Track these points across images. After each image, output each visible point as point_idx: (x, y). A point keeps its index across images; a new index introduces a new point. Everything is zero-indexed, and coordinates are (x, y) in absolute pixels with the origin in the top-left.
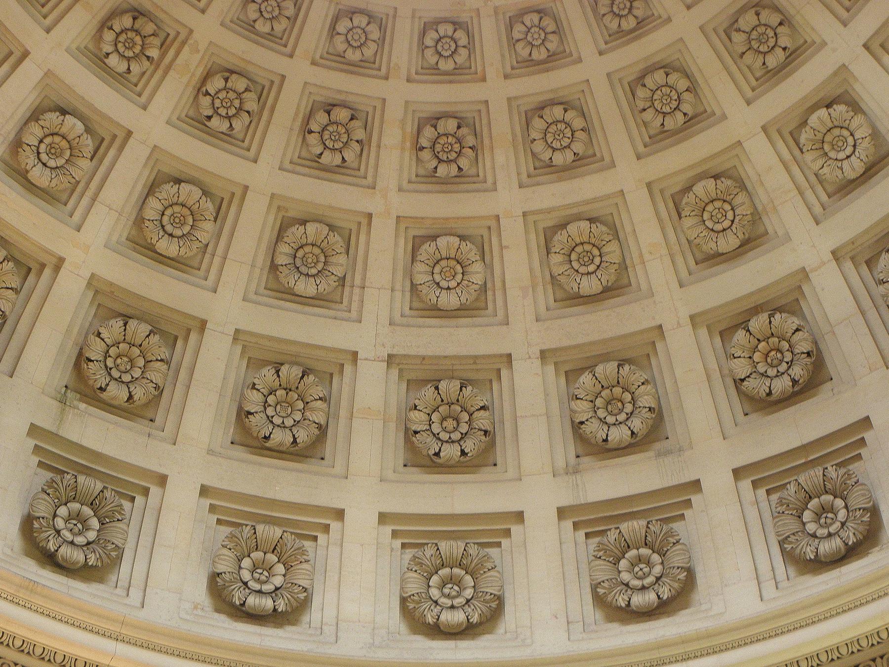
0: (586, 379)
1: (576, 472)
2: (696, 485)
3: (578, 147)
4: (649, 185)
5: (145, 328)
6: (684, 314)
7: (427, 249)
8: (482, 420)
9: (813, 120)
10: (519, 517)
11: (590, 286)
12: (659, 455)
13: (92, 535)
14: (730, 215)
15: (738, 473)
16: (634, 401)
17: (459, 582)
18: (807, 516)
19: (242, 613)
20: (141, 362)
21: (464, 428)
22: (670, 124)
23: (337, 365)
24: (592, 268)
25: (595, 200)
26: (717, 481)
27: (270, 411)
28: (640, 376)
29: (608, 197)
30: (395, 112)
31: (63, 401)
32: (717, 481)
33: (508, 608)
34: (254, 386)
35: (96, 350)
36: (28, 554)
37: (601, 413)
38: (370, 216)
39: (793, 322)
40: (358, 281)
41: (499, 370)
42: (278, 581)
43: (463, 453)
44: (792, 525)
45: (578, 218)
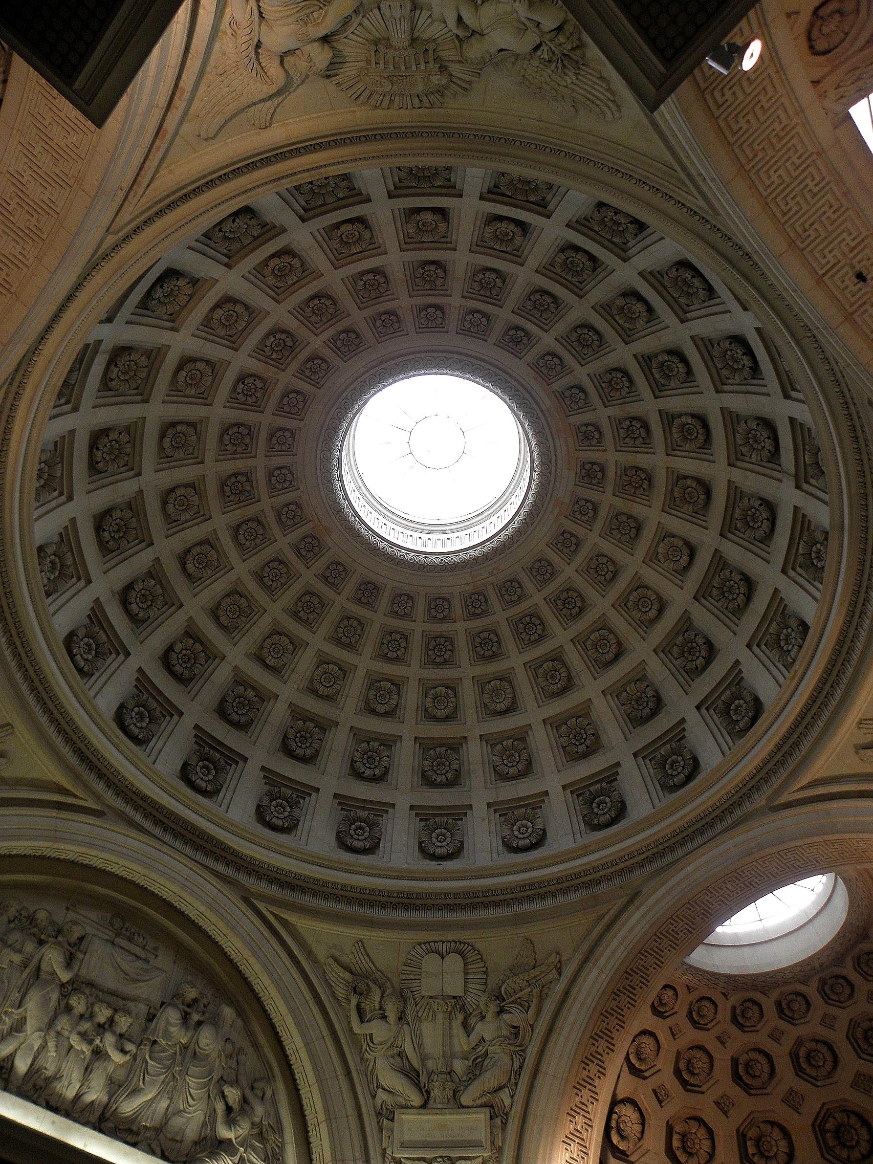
3: (248, 544)
9: (283, 638)
12: (132, 629)
14: (235, 616)
16: (148, 607)
22: (266, 580)
24: (197, 565)
25: (226, 556)
26: (133, 663)
29: (229, 562)
30: (251, 462)
38: (202, 462)
41: (144, 541)
43: (107, 542)
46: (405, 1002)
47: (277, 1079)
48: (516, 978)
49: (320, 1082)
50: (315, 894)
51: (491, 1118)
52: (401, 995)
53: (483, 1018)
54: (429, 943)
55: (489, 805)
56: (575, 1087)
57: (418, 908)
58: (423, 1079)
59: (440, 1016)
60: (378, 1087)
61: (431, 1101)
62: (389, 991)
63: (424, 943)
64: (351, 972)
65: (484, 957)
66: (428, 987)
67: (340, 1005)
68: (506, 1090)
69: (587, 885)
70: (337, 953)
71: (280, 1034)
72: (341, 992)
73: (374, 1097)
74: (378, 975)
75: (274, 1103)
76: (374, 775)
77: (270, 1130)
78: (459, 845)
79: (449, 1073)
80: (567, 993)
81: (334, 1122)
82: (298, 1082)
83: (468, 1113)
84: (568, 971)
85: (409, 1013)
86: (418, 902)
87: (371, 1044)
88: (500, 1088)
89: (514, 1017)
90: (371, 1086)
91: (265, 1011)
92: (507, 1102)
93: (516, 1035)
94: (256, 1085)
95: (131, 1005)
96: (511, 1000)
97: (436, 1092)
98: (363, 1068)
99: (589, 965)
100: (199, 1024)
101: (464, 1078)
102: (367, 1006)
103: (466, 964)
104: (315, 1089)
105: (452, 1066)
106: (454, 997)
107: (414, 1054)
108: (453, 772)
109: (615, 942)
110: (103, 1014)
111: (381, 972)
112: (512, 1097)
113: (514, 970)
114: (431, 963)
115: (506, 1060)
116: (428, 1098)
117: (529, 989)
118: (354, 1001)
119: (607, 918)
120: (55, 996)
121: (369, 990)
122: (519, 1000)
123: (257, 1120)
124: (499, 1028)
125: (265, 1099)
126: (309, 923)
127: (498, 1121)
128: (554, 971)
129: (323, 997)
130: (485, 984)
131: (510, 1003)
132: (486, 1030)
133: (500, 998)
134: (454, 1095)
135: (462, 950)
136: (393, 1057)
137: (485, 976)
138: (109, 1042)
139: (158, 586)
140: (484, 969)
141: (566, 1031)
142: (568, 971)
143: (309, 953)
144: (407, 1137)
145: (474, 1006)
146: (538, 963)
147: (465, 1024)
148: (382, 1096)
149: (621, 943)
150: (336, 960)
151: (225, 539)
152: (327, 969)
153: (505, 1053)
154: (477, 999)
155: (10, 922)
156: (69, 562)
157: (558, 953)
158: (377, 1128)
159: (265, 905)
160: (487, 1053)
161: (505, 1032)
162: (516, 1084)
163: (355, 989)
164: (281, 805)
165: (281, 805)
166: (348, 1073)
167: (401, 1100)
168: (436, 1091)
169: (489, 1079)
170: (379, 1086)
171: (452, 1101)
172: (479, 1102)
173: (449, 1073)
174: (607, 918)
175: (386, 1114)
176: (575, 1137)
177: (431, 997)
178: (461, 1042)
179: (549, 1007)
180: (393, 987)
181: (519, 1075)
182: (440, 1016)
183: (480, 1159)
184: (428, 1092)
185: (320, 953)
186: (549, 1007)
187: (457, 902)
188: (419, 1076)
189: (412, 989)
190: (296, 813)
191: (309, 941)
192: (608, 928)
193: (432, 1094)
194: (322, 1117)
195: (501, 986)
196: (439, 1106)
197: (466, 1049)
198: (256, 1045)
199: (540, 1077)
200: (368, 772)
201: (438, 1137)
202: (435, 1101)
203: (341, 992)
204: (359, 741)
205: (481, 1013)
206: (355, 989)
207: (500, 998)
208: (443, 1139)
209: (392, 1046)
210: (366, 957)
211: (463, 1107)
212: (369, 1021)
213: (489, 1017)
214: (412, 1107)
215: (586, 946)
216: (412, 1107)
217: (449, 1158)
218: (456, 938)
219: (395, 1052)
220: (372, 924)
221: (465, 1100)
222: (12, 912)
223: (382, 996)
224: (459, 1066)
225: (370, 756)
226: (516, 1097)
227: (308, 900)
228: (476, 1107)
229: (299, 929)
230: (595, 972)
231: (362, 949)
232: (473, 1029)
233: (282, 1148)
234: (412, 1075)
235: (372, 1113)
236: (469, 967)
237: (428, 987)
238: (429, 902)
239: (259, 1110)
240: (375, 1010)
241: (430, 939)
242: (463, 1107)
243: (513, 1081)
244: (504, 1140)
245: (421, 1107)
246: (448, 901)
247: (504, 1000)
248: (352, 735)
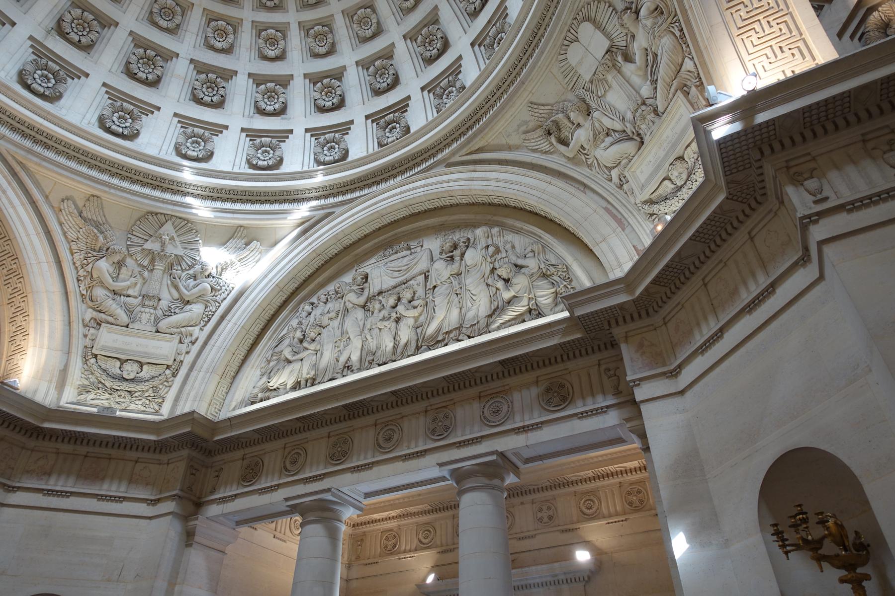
0: (263, 87)
1: (252, 117)
2: (291, 131)
4: (299, 23)
5: (91, 17)
6: (302, 72)
7: (213, 23)
8: (222, 91)
10: (226, 127)
11: (271, 54)
13: (50, 85)
15: (307, 130)
17: (199, 144)
18: (325, 148)
19: (108, 130)
20: (88, 30)
21: (215, 93)
23: (169, 56)
26: (299, 131)
27: (140, 65)
28: (282, 90)
31: (49, 32)
32: (299, 131)
33: (214, 156)
34: (134, 54)
35: (68, 18)
36: (19, 83)
37: (266, 100)
39: (338, 83)
40: (184, 28)
42: (128, 124)
44: (320, 150)
45: (272, 28)
67: (551, 153)
70: (524, 128)
72: (545, 146)
95: (412, 282)
100: (463, 255)
110: (392, 301)
120: (360, 314)
138: (401, 308)
139: (268, 84)
151: (264, 17)
155: (325, 303)
156: (201, 131)
182: (609, 78)
185: (515, 140)
191: (504, 142)
198: (518, 231)
203: (545, 146)
222: (323, 298)
229: (492, 143)
234: (626, 137)
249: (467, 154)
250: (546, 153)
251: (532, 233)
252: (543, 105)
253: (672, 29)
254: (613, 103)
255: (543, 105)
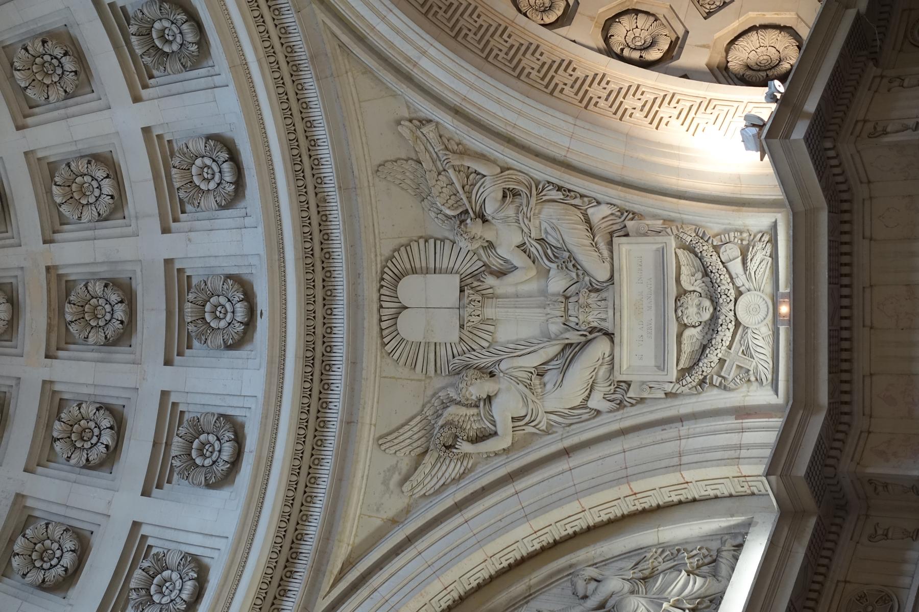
46: (467, 367)
47: (574, 561)
48: (435, 191)
49: (577, 495)
50: (304, 518)
51: (627, 235)
52: (458, 374)
53: (490, 246)
54: (382, 330)
55: (166, 230)
56: (586, 107)
57: (329, 349)
58: (574, 337)
59: (489, 312)
60: (587, 408)
61: (604, 325)
62: (453, 394)
63: (382, 337)
64: (426, 452)
65: (404, 241)
66: (446, 331)
68: (590, 211)
69: (295, 70)
70: (396, 478)
71: (512, 561)
72: (453, 469)
73: (598, 412)
74: (429, 412)
75: (606, 562)
76: (111, 428)
77: (640, 567)
78: (230, 282)
79: (567, 298)
80: (457, 112)
81: (630, 471)
82: (577, 529)
83: (620, 270)
84: (427, 109)
85: (485, 361)
86: (319, 348)
87: (527, 419)
88: (588, 221)
89: (490, 196)
90: (585, 417)
91: (479, 587)
92: (605, 210)
93: (516, 194)
94: (581, 593)
96: (465, 200)
97: (593, 319)
98: (560, 431)
99: (416, 73)
101: (574, 275)
102: (473, 427)
103: (414, 271)
104: (587, 502)
105: (558, 294)
106: (462, 290)
107: (541, 351)
108: (108, 291)
109: (382, 27)
111: (424, 406)
112: (599, 203)
113: (422, 195)
114: (411, 327)
115: (549, 211)
116: (600, 330)
117: (451, 171)
118: (465, 447)
119: (345, 38)
121: (449, 424)
122: (467, 188)
123: (627, 586)
124: (505, 220)
125: (600, 578)
126: (349, 525)
127: (630, 224)
128: (425, 130)
129: (459, 496)
130: (443, 241)
131: (470, 202)
132: (507, 240)
133: (462, 218)
134: (597, 291)
135: (392, 277)
136: (545, 385)
137: (432, 241)
140: (422, 242)
141: (511, 117)
142: (427, 109)
143: (394, 522)
144: (650, 361)
145: (475, 258)
146: (413, 156)
147: (500, 274)
148: (596, 402)
149: (383, 18)
150: (406, 479)
152: (420, 491)
153: (539, 213)
154: (463, 254)
157: (398, 123)
158: (639, 406)
159: (319, 600)
160: (541, 240)
161: (510, 211)
162: (582, 196)
163: (448, 448)
164: (160, 586)
165: (160, 586)
166: (566, 452)
167: (603, 371)
168: (590, 318)
169: (575, 238)
170: (583, 406)
171: (604, 295)
172: (606, 253)
173: (567, 298)
174: (345, 38)
175: (621, 393)
176: (650, 110)
177: (462, 327)
178: (523, 280)
179: (477, 141)
180: (443, 388)
181: (569, 191)
182: (489, 312)
183: (680, 252)
184: (593, 330)
185: (394, 504)
186: (477, 141)
187: (319, 283)
188: (571, 344)
189: (450, 357)
190: (173, 559)
191: (378, 523)
192: (361, 39)
193: (595, 324)
194: (625, 490)
195: (446, 216)
196: (611, 312)
197: (533, 273)
199: (574, 159)
200: (107, 438)
201: (650, 316)
202: (604, 320)
204: (51, 458)
205: (484, 248)
206: (448, 448)
207: (462, 218)
208: (653, 308)
209: (529, 387)
210: (401, 431)
211: (612, 277)
212: (494, 423)
213: (489, 235)
214: (612, 355)
215: (388, 78)
216: (612, 355)
217: (677, 299)
218: (375, 286)
219: (537, 382)
220: (350, 422)
221: (601, 273)
223: (459, 403)
224: (557, 283)
225: (79, 435)
226: (599, 197)
227: (314, 530)
228: (612, 259)
229: (358, 540)
230: (425, 63)
231: (389, 438)
232: (506, 261)
233: (663, 547)
235: (619, 414)
236: (418, 266)
237: (446, 331)
238: (320, 330)
239: (614, 584)
240: (479, 414)
241: (376, 329)
242: (612, 277)
243: (577, 201)
244: (655, 217)
245: (612, 341)
246: (319, 299)
247: (466, 212)
248: (40, 469)
249: (333, 586)
250: (462, 476)
251: (551, 576)
252: (403, 426)
253: (545, 198)
254: (514, 338)
255: (403, 426)
